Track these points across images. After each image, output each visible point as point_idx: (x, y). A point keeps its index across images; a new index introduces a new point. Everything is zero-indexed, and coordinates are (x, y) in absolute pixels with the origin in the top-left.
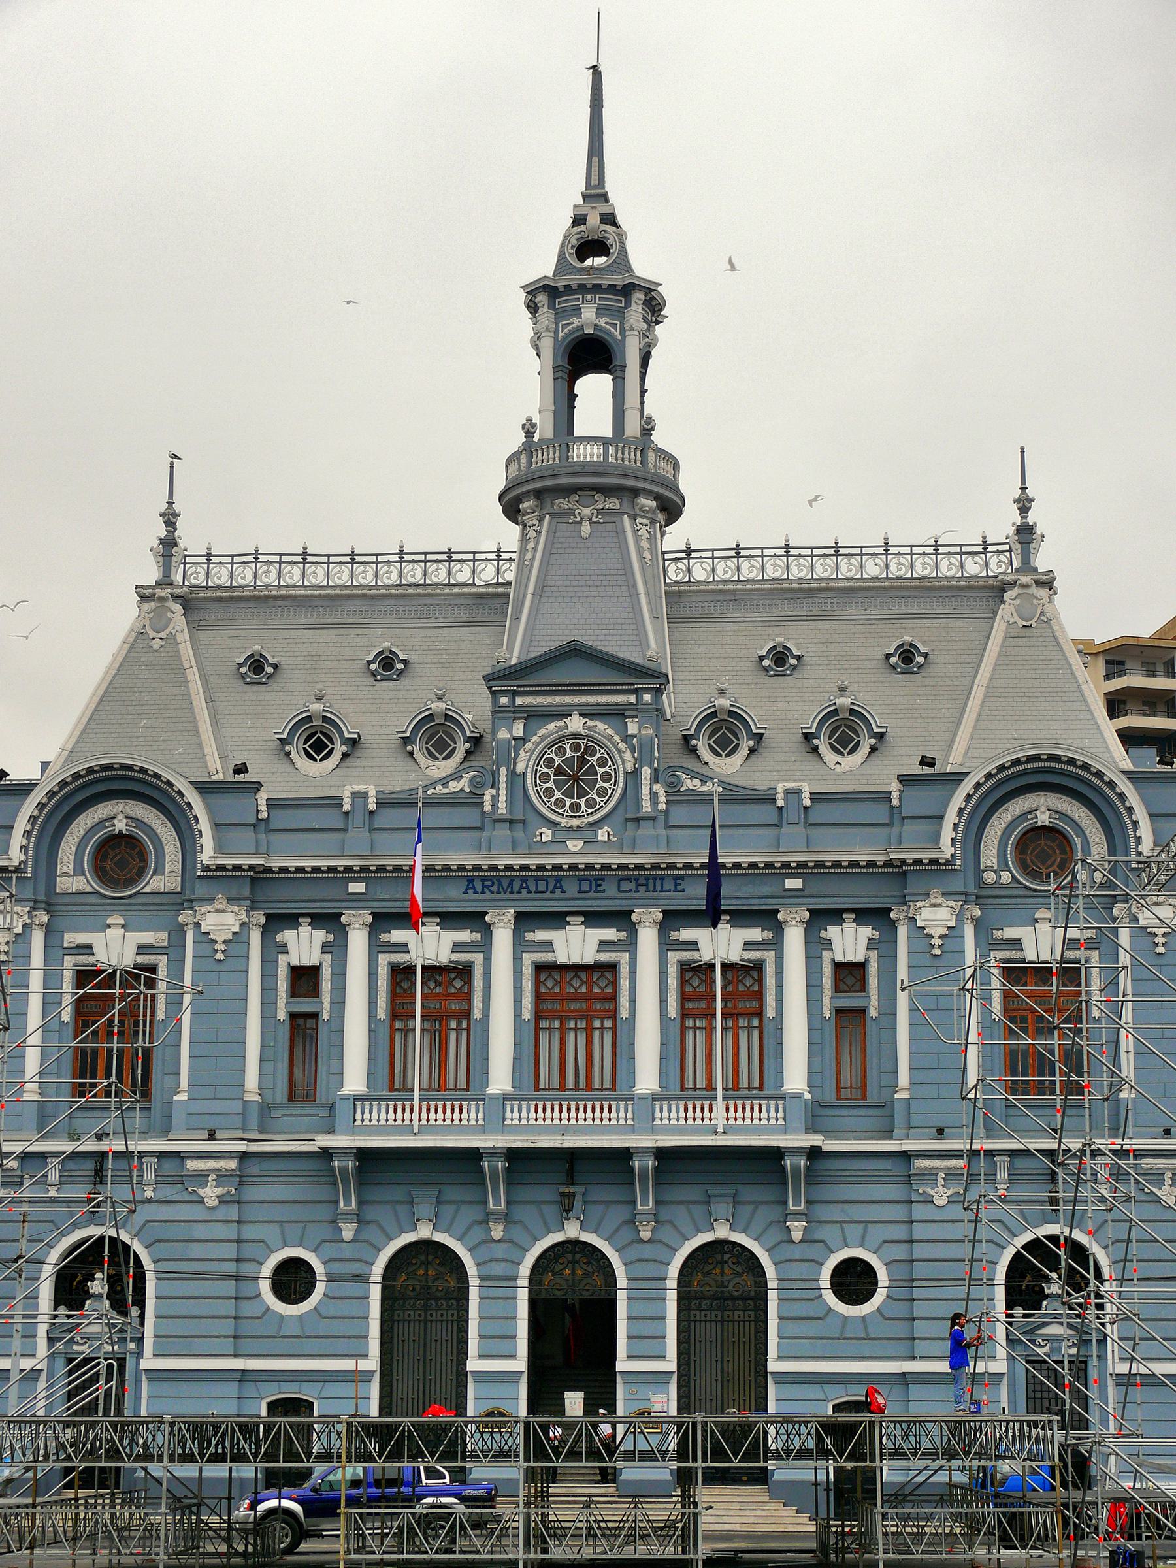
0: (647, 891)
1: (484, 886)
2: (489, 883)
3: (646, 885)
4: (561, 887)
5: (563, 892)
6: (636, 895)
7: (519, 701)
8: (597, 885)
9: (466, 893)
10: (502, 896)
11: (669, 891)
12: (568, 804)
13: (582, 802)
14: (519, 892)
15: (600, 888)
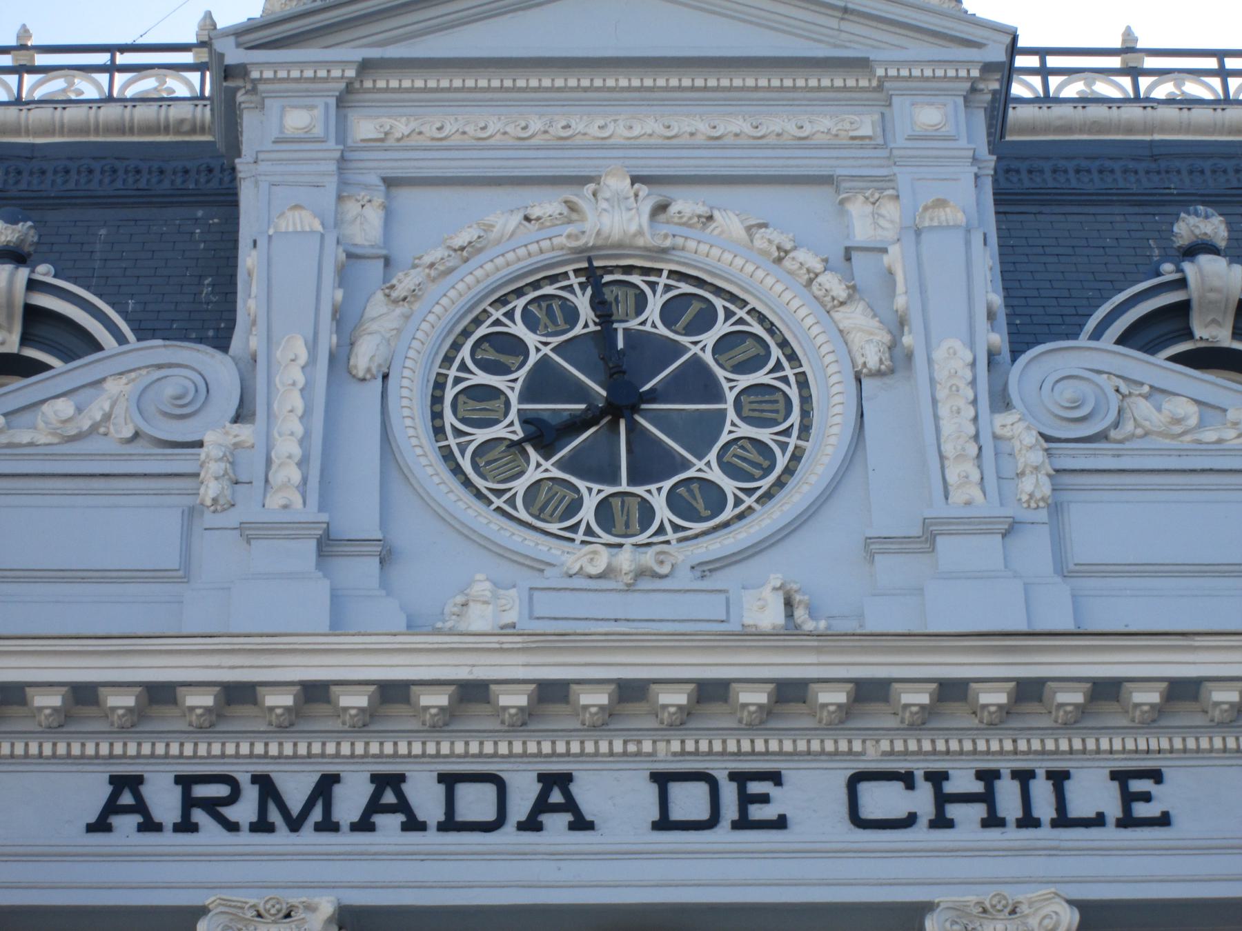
0: (993, 821)
1: (189, 803)
2: (222, 791)
3: (988, 798)
4: (570, 805)
5: (581, 824)
6: (942, 836)
7: (364, 127)
8: (746, 800)
9: (100, 825)
10: (282, 838)
11: (1099, 821)
12: (590, 505)
13: (657, 495)
14: (364, 825)
15: (757, 812)
